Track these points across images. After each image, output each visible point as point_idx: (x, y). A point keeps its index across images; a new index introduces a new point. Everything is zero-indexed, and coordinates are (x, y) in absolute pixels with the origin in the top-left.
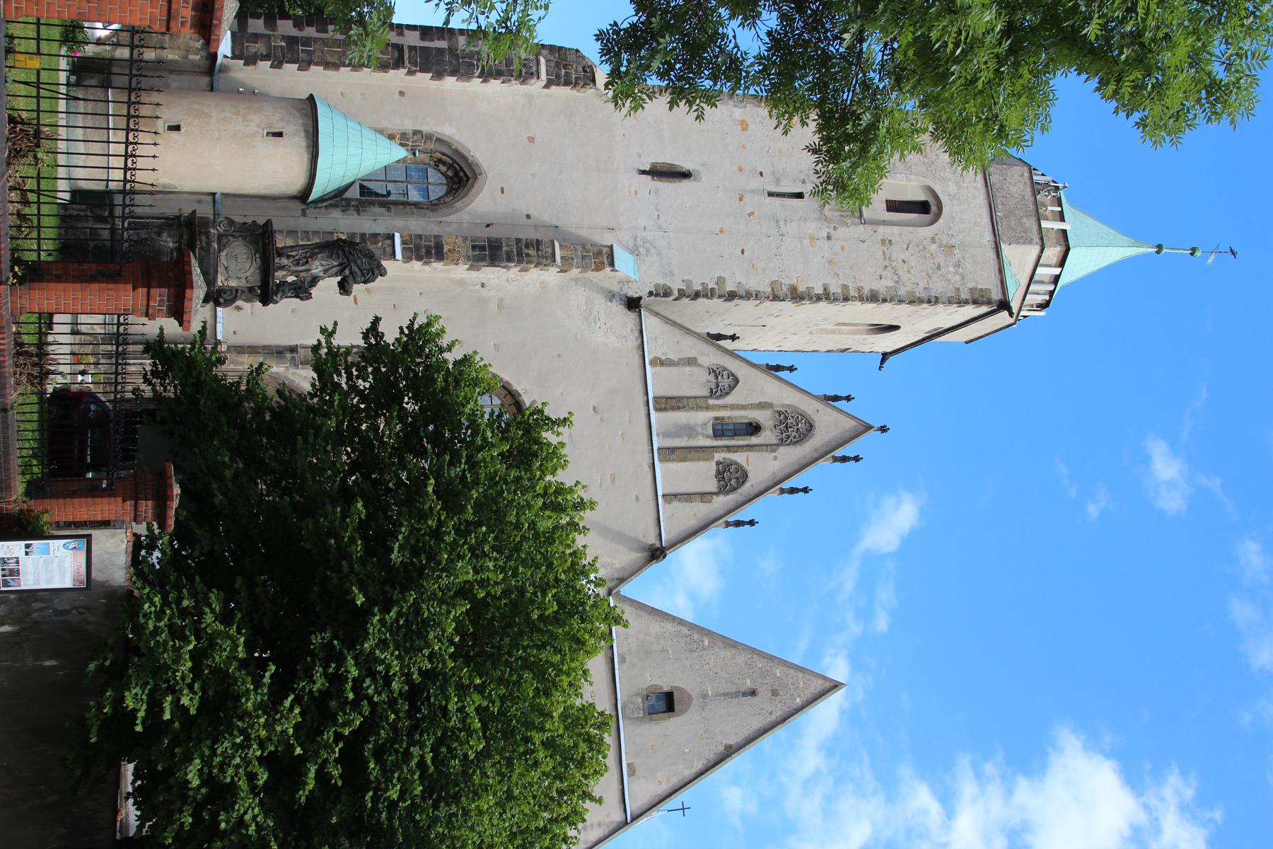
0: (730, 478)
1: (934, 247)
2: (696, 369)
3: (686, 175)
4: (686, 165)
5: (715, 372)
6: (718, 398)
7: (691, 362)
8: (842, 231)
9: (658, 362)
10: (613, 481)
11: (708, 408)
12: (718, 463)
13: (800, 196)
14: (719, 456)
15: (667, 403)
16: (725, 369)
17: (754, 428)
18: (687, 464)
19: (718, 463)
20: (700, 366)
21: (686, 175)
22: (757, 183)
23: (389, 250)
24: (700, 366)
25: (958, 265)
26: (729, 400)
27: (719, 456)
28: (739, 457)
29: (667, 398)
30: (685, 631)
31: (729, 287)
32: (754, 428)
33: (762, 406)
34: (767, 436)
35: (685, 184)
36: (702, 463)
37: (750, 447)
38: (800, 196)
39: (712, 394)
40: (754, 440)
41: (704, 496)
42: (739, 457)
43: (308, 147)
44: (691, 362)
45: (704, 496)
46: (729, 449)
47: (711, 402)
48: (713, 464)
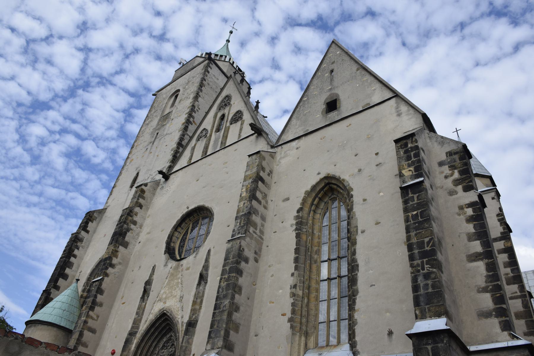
0: (238, 117)
1: (187, 87)
3: (138, 174)
4: (134, 175)
8: (172, 117)
10: (226, 163)
11: (211, 136)
12: (231, 124)
13: (157, 134)
14: (228, 124)
16: (199, 135)
21: (138, 174)
22: (149, 150)
23: (97, 283)
24: (195, 145)
25: (193, 77)
30: (298, 109)
31: (175, 146)
32: (223, 116)
35: (140, 174)
38: (157, 134)
40: (226, 115)
41: (242, 124)
43: (35, 326)
44: (193, 149)
45: (242, 124)
47: (208, 135)
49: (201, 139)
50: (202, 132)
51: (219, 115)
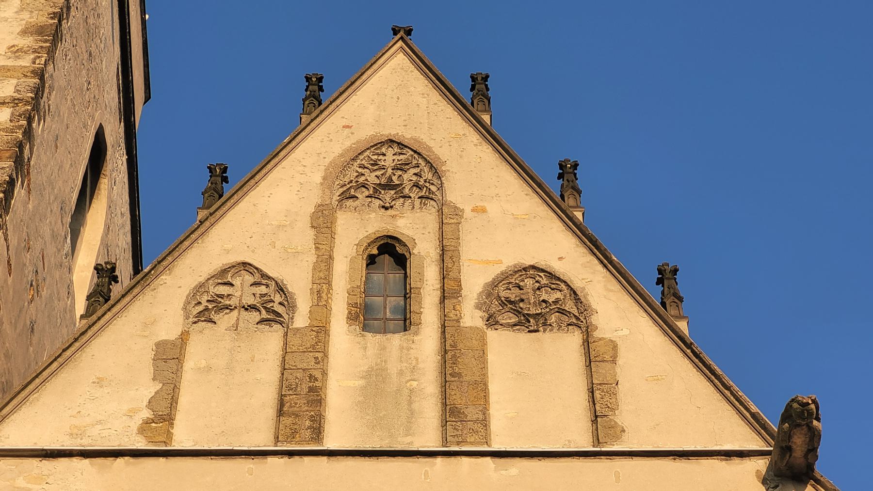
2: (195, 357)
5: (208, 307)
6: (289, 303)
7: (169, 358)
9: (164, 414)
12: (492, 321)
14: (471, 317)
15: (300, 405)
16: (201, 288)
17: (389, 252)
18: (493, 387)
19: (492, 321)
20: (184, 337)
24: (184, 337)
26: (298, 280)
27: (471, 317)
28: (474, 281)
29: (280, 412)
33: (323, 223)
34: (415, 226)
36: (491, 357)
37: (447, 256)
39: (273, 318)
40: (424, 249)
41: (595, 356)
42: (474, 281)
44: (169, 358)
45: (595, 356)
46: (449, 293)
47: (301, 320)
48: (493, 336)
49: (226, 320)
50: (223, 276)
51: (356, 229)
